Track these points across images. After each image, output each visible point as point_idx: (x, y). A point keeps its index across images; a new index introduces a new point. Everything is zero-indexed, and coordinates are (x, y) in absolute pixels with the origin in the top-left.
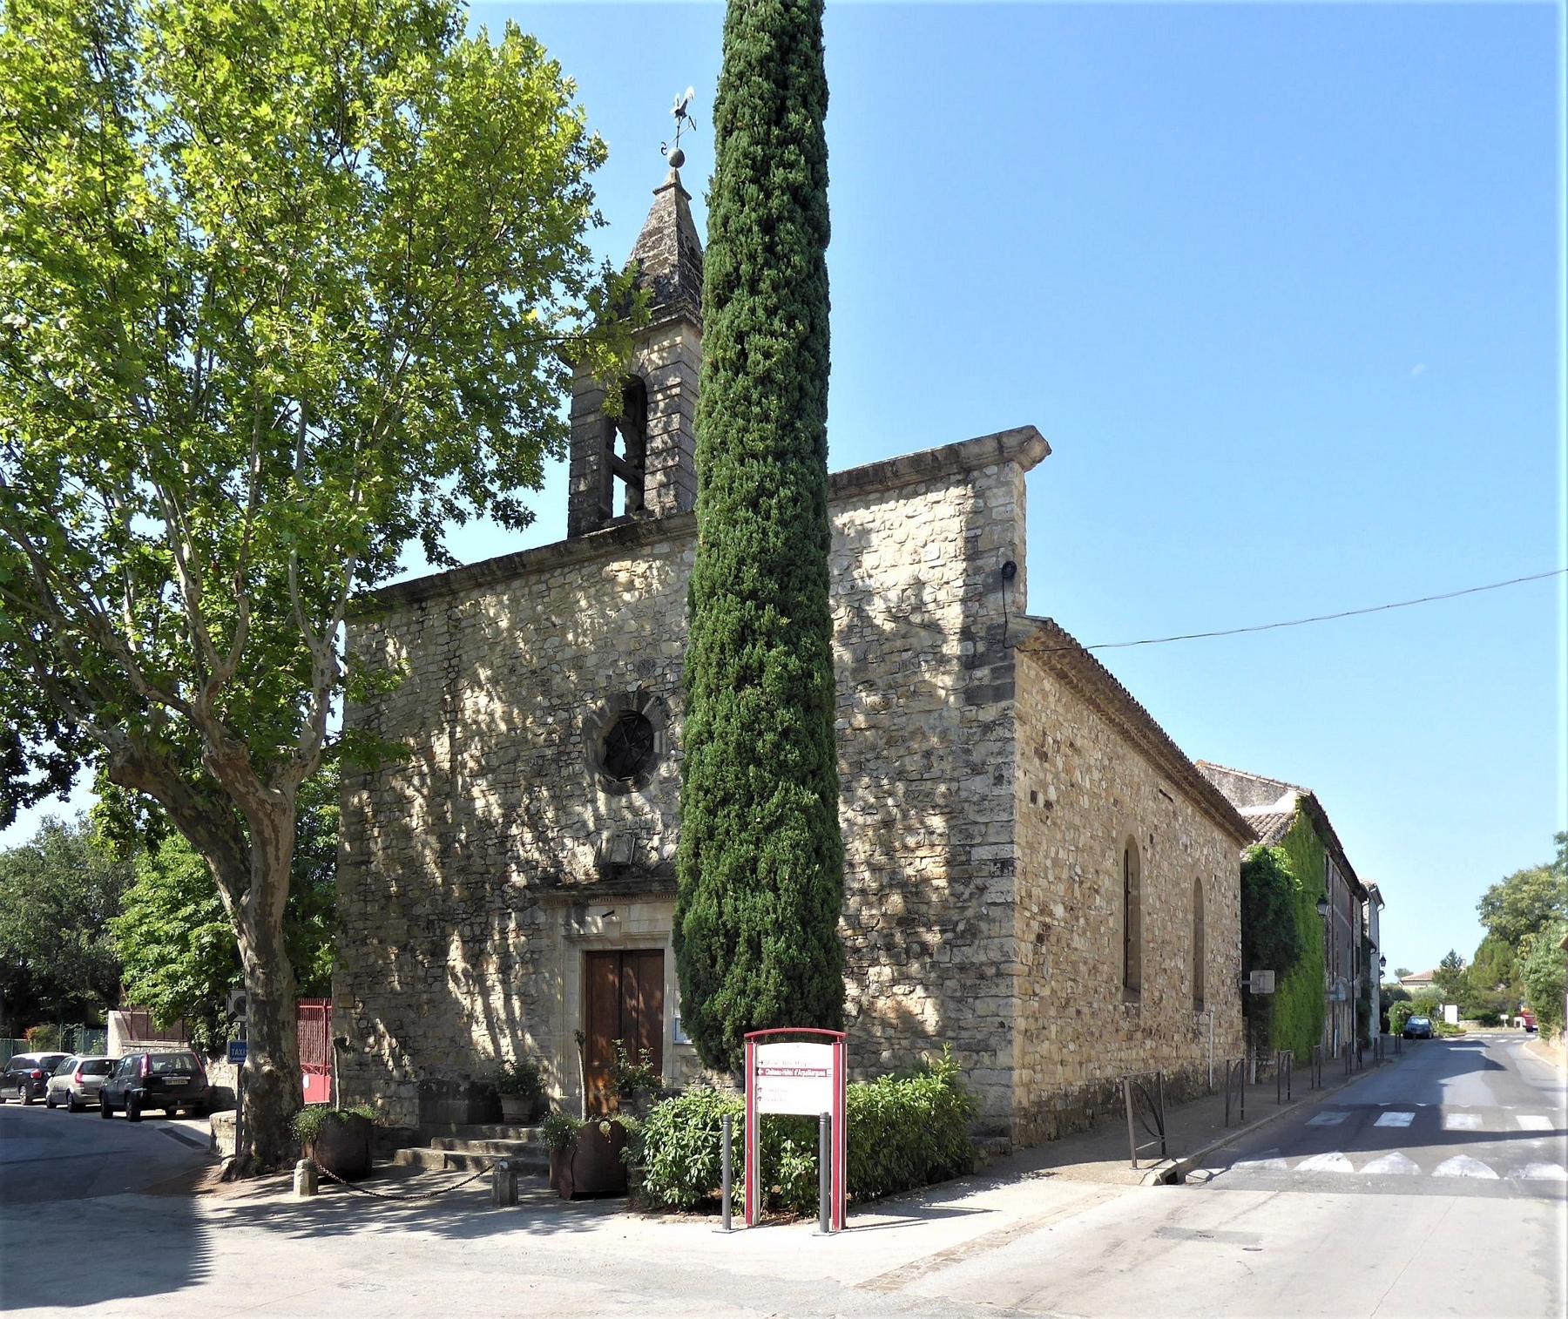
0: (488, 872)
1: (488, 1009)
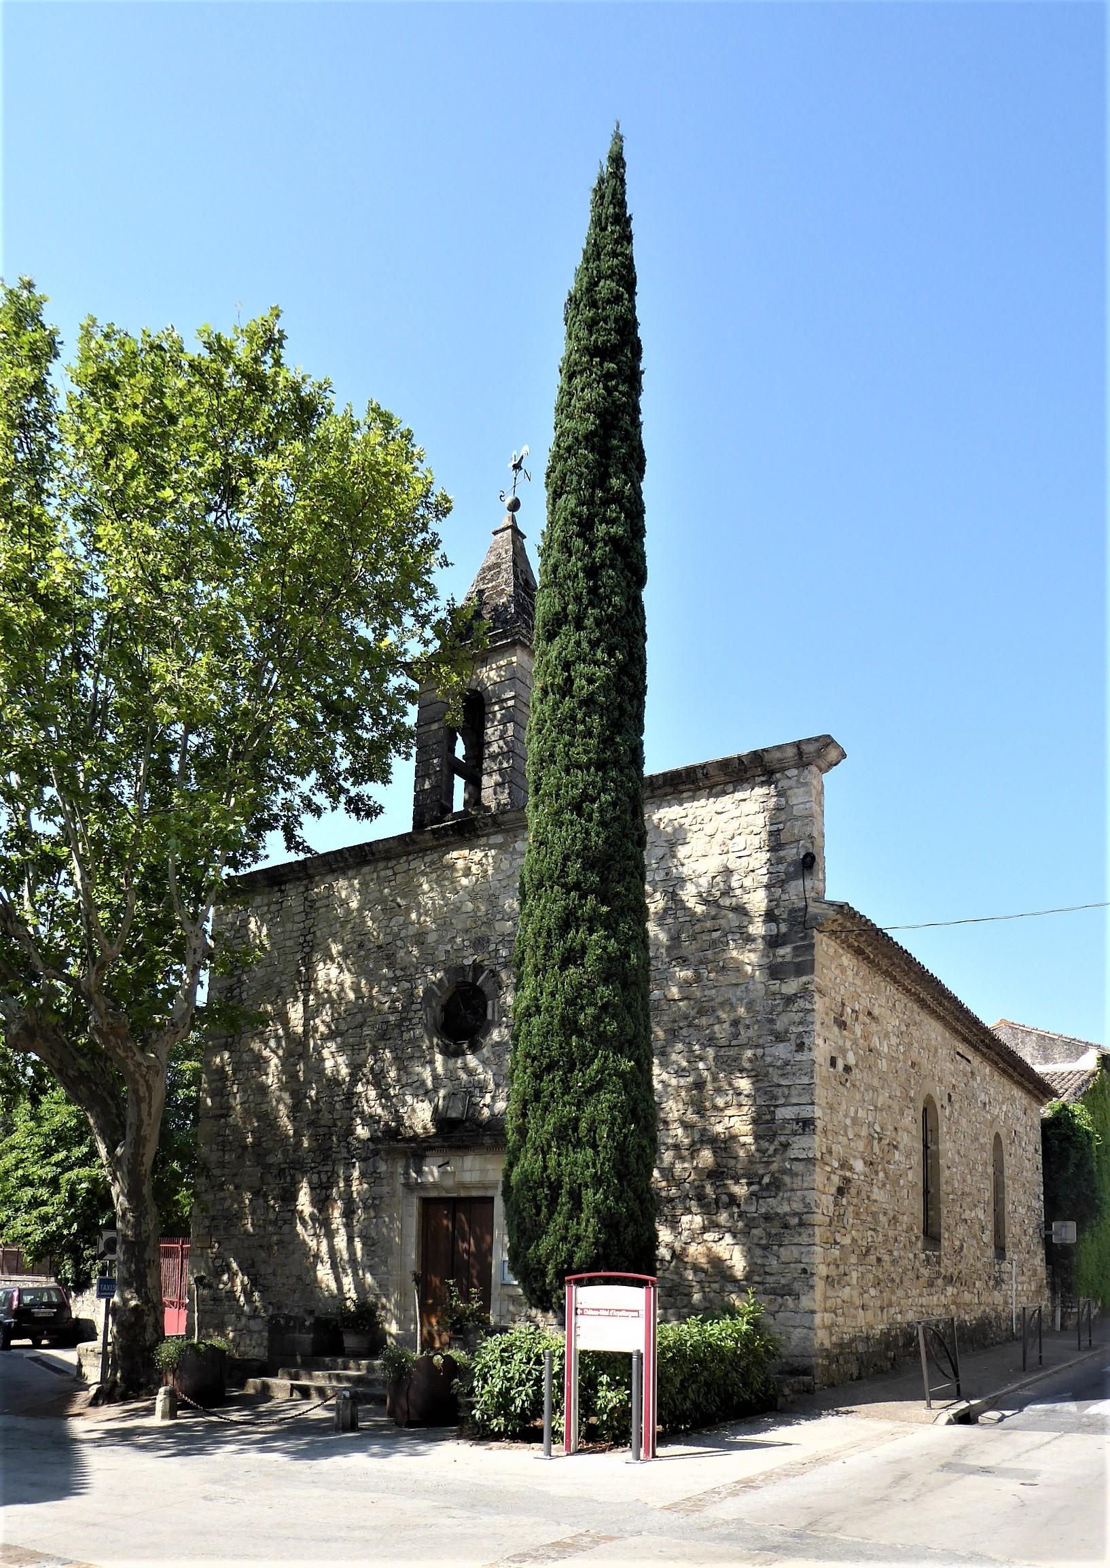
0: (335, 1126)
1: (332, 1250)
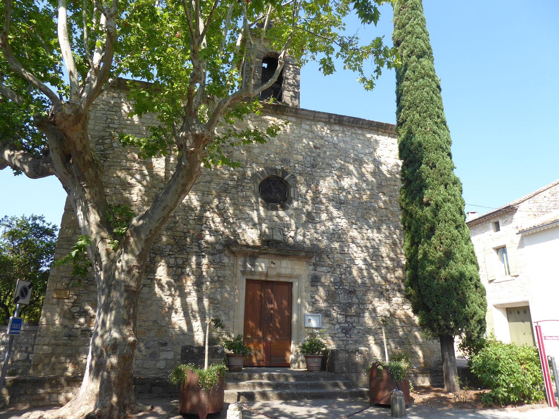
0: (189, 232)
1: (185, 306)
